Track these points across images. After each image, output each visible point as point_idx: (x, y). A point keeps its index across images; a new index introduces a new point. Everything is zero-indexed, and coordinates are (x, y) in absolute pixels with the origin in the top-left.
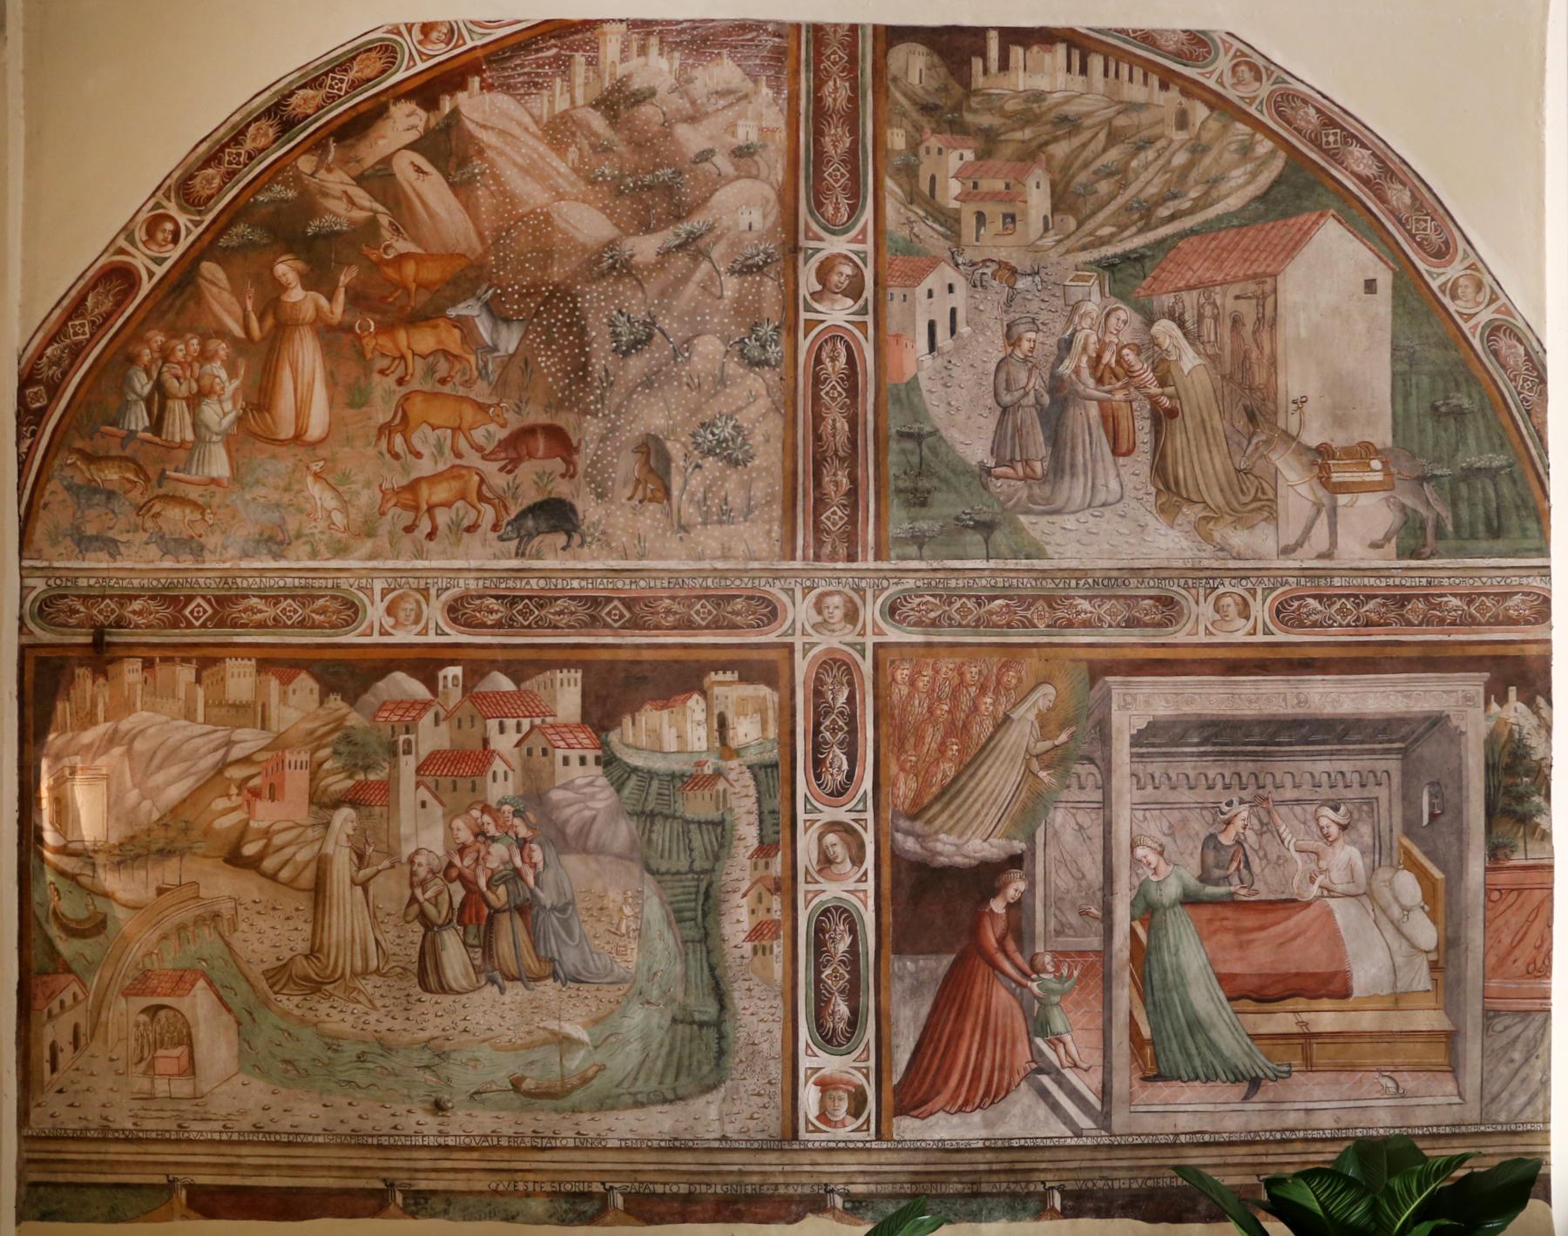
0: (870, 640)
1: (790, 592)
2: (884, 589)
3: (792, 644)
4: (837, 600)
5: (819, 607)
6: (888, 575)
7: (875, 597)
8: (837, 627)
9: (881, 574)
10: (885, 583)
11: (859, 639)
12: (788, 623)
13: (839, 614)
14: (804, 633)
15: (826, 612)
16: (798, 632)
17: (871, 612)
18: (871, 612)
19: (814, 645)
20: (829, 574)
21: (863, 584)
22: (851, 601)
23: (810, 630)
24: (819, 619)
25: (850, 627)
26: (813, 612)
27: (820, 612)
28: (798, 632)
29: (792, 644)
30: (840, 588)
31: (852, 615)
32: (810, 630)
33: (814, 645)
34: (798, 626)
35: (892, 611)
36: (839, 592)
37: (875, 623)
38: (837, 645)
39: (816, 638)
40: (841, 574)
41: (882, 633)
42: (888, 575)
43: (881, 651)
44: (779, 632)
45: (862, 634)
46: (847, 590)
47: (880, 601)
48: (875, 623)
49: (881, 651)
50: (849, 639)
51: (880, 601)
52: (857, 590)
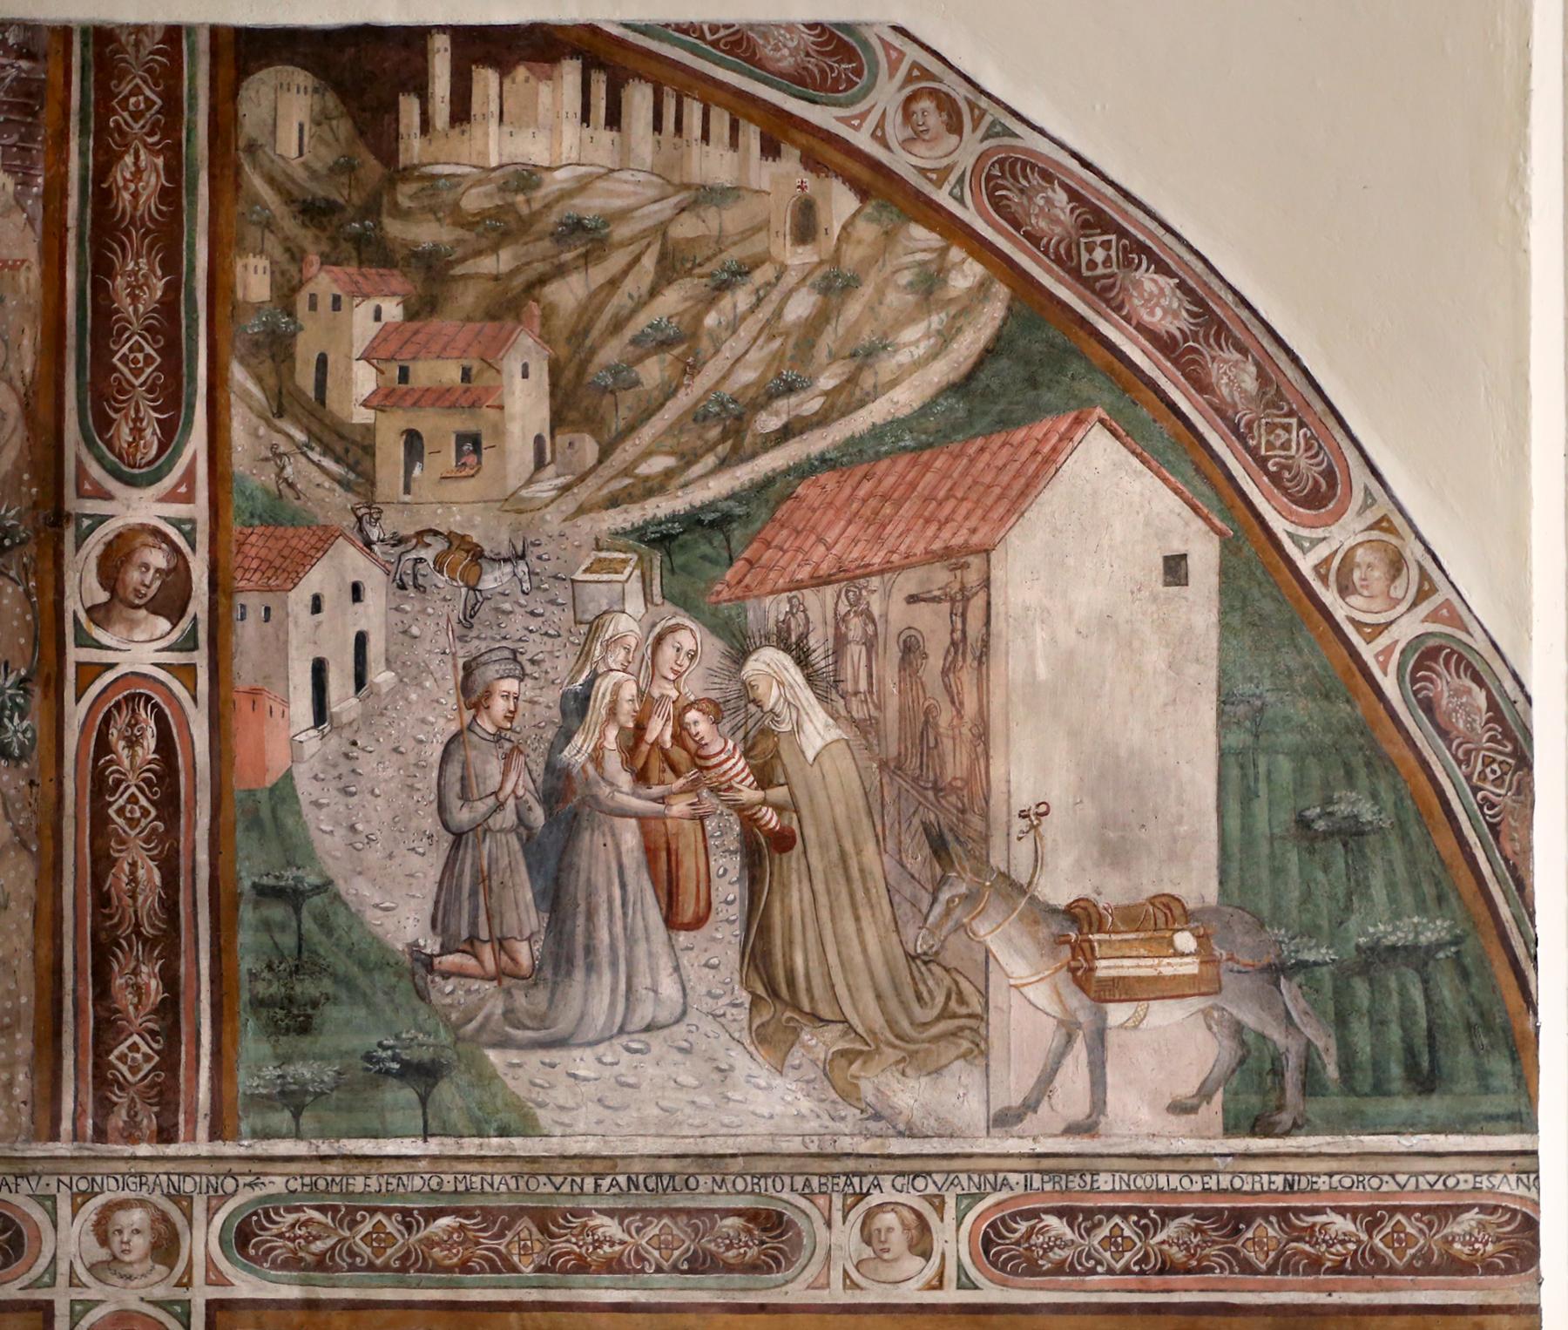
0: (200, 1294)
1: (48, 1203)
2: (228, 1196)
3: (50, 1303)
4: (137, 1216)
5: (102, 1231)
6: (236, 1167)
7: (211, 1212)
8: (137, 1269)
9: (223, 1167)
10: (230, 1184)
11: (180, 1294)
12: (44, 1261)
13: (140, 1244)
14: (73, 1281)
15: (116, 1240)
16: (62, 1280)
17: (203, 1240)
18: (203, 1240)
19: (91, 1304)
20: (122, 1167)
21: (188, 1186)
22: (165, 1218)
23: (84, 1276)
24: (102, 1254)
25: (161, 1269)
26: (91, 1240)
27: (104, 1241)
28: (62, 1280)
29: (50, 1303)
30: (144, 1193)
31: (166, 1247)
32: (84, 1276)
33: (91, 1304)
34: (63, 1267)
35: (242, 1238)
36: (141, 1203)
37: (209, 1261)
38: (133, 1304)
39: (93, 1293)
40: (145, 1167)
41: (223, 1282)
42: (236, 1167)
43: (220, 1316)
44: (26, 1280)
45: (185, 1283)
46: (157, 1198)
47: (219, 1220)
48: (209, 1261)
49: (220, 1316)
50: (160, 1292)
51: (219, 1220)
52: (177, 1197)
